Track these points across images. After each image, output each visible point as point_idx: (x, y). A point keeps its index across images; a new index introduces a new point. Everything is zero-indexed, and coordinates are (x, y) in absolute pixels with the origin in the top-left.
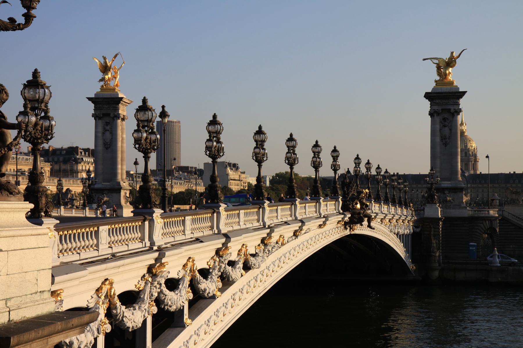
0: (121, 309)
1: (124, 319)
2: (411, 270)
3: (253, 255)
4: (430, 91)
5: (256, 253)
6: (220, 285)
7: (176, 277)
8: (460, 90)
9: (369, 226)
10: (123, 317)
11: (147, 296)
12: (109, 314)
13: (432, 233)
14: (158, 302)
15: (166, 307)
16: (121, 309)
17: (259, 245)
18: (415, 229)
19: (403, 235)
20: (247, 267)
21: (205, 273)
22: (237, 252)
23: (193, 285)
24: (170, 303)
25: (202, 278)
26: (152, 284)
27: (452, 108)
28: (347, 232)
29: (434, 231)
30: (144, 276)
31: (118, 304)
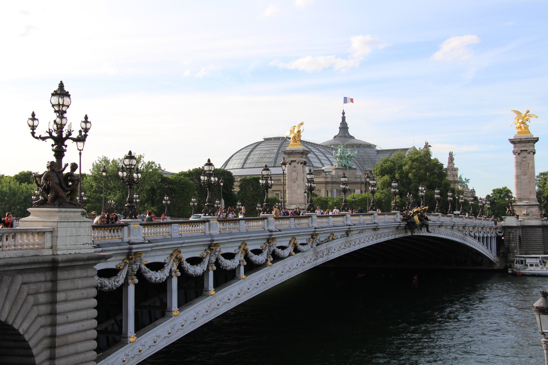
0: (187, 265)
1: (189, 270)
2: (495, 262)
3: (303, 244)
4: (513, 138)
5: (307, 243)
6: (272, 259)
7: (234, 252)
8: (534, 137)
9: (428, 231)
10: (188, 269)
11: (206, 261)
12: (180, 267)
13: (511, 236)
14: (217, 263)
15: (224, 268)
16: (187, 265)
17: (309, 239)
18: (499, 234)
19: (483, 237)
20: (296, 250)
21: (257, 252)
22: (289, 242)
23: (246, 257)
24: (225, 265)
25: (253, 254)
26: (210, 254)
27: (530, 149)
28: (409, 234)
29: (513, 235)
30: (206, 250)
31: (185, 262)
